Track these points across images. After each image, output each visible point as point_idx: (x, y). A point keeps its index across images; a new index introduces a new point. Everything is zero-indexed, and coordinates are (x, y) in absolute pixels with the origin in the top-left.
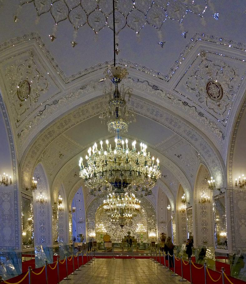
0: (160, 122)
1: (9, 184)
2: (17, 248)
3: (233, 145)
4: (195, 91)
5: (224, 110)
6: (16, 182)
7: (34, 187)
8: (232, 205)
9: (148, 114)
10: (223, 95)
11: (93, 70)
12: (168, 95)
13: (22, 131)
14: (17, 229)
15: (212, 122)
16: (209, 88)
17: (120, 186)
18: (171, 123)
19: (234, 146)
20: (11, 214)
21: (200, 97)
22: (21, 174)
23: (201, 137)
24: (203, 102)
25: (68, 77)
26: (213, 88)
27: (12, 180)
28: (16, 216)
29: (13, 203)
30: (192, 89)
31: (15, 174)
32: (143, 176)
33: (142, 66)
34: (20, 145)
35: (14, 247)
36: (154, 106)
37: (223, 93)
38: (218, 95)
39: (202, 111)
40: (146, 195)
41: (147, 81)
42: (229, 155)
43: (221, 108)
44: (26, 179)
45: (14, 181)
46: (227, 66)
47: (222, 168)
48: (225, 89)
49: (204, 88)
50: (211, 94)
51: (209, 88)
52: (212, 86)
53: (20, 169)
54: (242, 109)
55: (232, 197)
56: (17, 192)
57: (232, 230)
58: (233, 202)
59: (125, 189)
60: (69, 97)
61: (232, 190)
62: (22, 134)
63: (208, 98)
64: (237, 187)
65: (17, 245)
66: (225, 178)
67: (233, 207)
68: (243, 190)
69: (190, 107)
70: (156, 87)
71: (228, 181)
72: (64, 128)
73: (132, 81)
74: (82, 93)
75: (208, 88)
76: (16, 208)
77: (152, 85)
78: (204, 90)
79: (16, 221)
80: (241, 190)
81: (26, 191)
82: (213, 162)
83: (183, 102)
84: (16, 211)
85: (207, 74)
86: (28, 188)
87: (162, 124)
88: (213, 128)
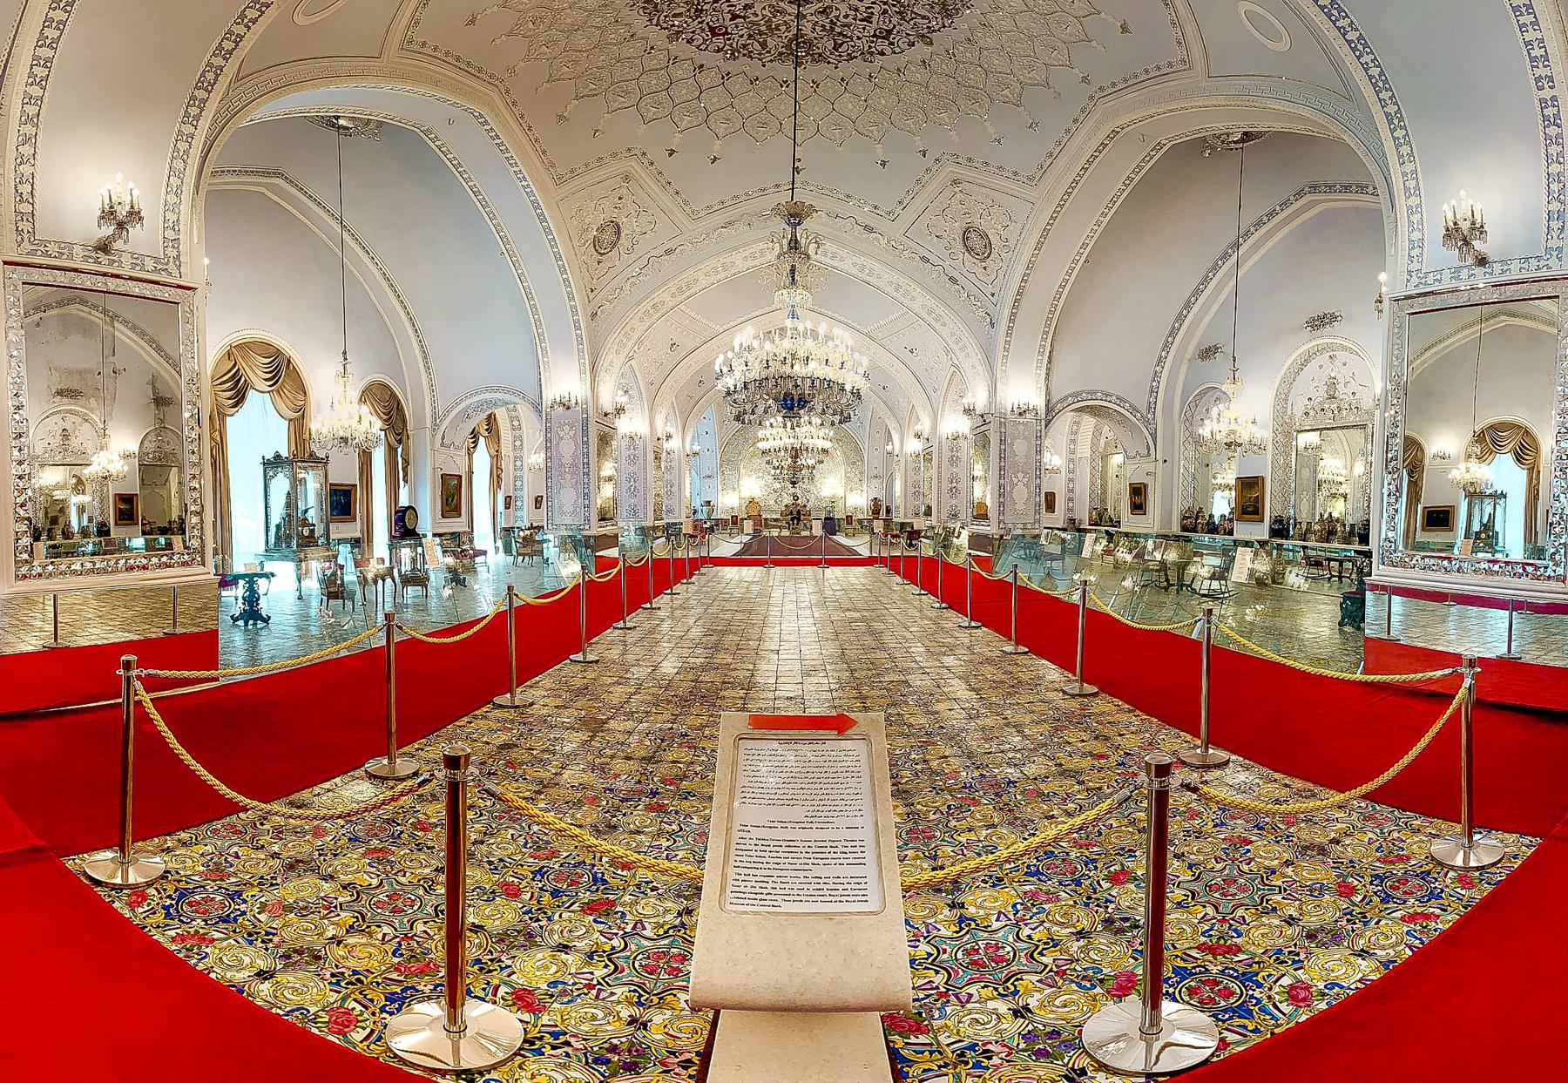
3: (1008, 339)
7: (620, 410)
9: (854, 272)
12: (893, 243)
17: (793, 405)
18: (897, 291)
29: (580, 442)
32: (836, 388)
39: (956, 275)
40: (840, 422)
49: (958, 236)
52: (973, 235)
59: (802, 412)
72: (684, 296)
75: (965, 239)
78: (959, 240)
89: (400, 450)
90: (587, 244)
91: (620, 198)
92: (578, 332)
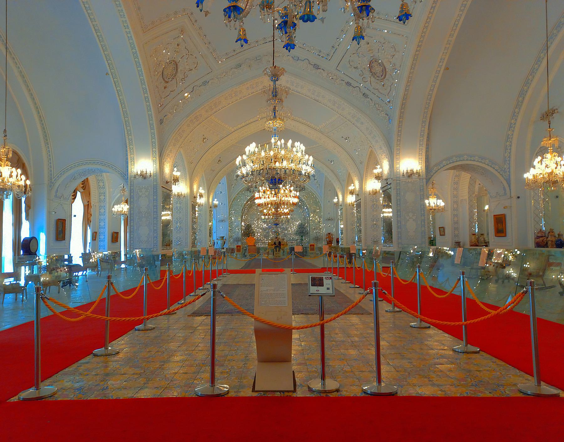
0: (323, 103)
1: (149, 177)
2: (155, 249)
4: (358, 70)
5: (388, 90)
6: (156, 175)
7: (176, 180)
8: (398, 198)
10: (386, 73)
11: (250, 47)
13: (164, 117)
14: (155, 228)
15: (377, 104)
16: (372, 66)
19: (401, 130)
20: (149, 211)
21: (364, 76)
22: (162, 165)
23: (366, 121)
24: (367, 82)
25: (221, 55)
26: (376, 66)
27: (152, 172)
28: (155, 213)
30: (354, 68)
31: (155, 165)
33: (303, 43)
34: (162, 132)
35: (151, 249)
36: (315, 87)
37: (386, 72)
38: (381, 74)
39: (367, 92)
41: (307, 59)
42: (396, 140)
43: (385, 88)
44: (167, 170)
45: (153, 175)
46: (387, 41)
47: (389, 156)
48: (389, 67)
50: (374, 73)
51: (372, 66)
52: (374, 64)
53: (161, 160)
54: (407, 88)
55: (399, 189)
56: (156, 186)
57: (398, 225)
58: (400, 193)
60: (221, 77)
61: (399, 180)
62: (164, 121)
63: (372, 77)
64: (405, 177)
65: (155, 246)
66: (392, 166)
67: (400, 200)
68: (412, 180)
69: (354, 87)
70: (316, 66)
71: (395, 171)
73: (291, 59)
74: (236, 73)
75: (371, 67)
76: (155, 204)
77: (313, 64)
79: (155, 219)
80: (410, 180)
81: (166, 185)
82: (381, 148)
83: (347, 82)
84: (155, 207)
85: (368, 51)
86: (169, 181)
87: (325, 105)
88: (378, 111)
89: (23, 199)
90: (159, 75)
91: (178, 45)
92: (152, 131)
